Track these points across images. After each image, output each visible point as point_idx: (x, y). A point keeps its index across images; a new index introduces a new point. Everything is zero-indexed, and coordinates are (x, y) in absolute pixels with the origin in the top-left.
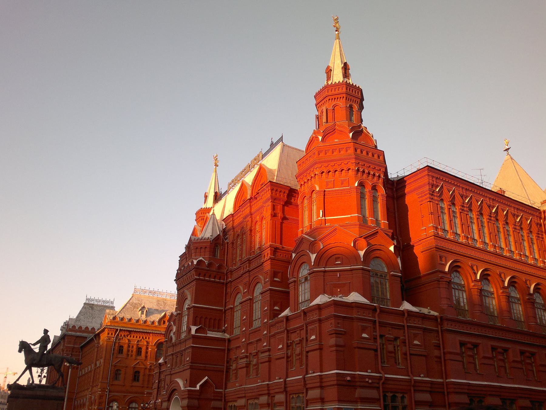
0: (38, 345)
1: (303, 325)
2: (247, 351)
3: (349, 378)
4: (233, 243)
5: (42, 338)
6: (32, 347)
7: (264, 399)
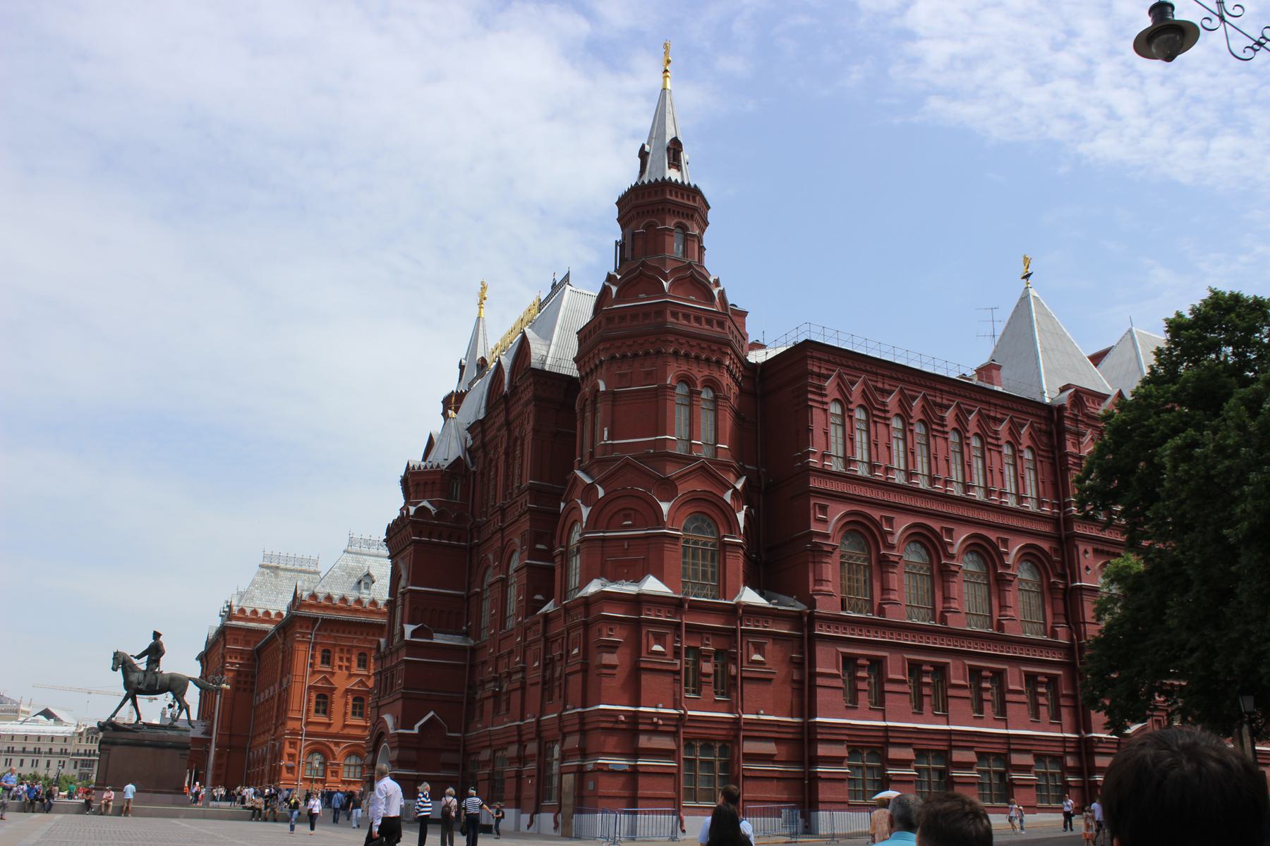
0: (146, 658)
1: (562, 633)
2: (496, 670)
3: (623, 718)
4: (482, 474)
5: (151, 646)
6: (136, 661)
7: (513, 750)
